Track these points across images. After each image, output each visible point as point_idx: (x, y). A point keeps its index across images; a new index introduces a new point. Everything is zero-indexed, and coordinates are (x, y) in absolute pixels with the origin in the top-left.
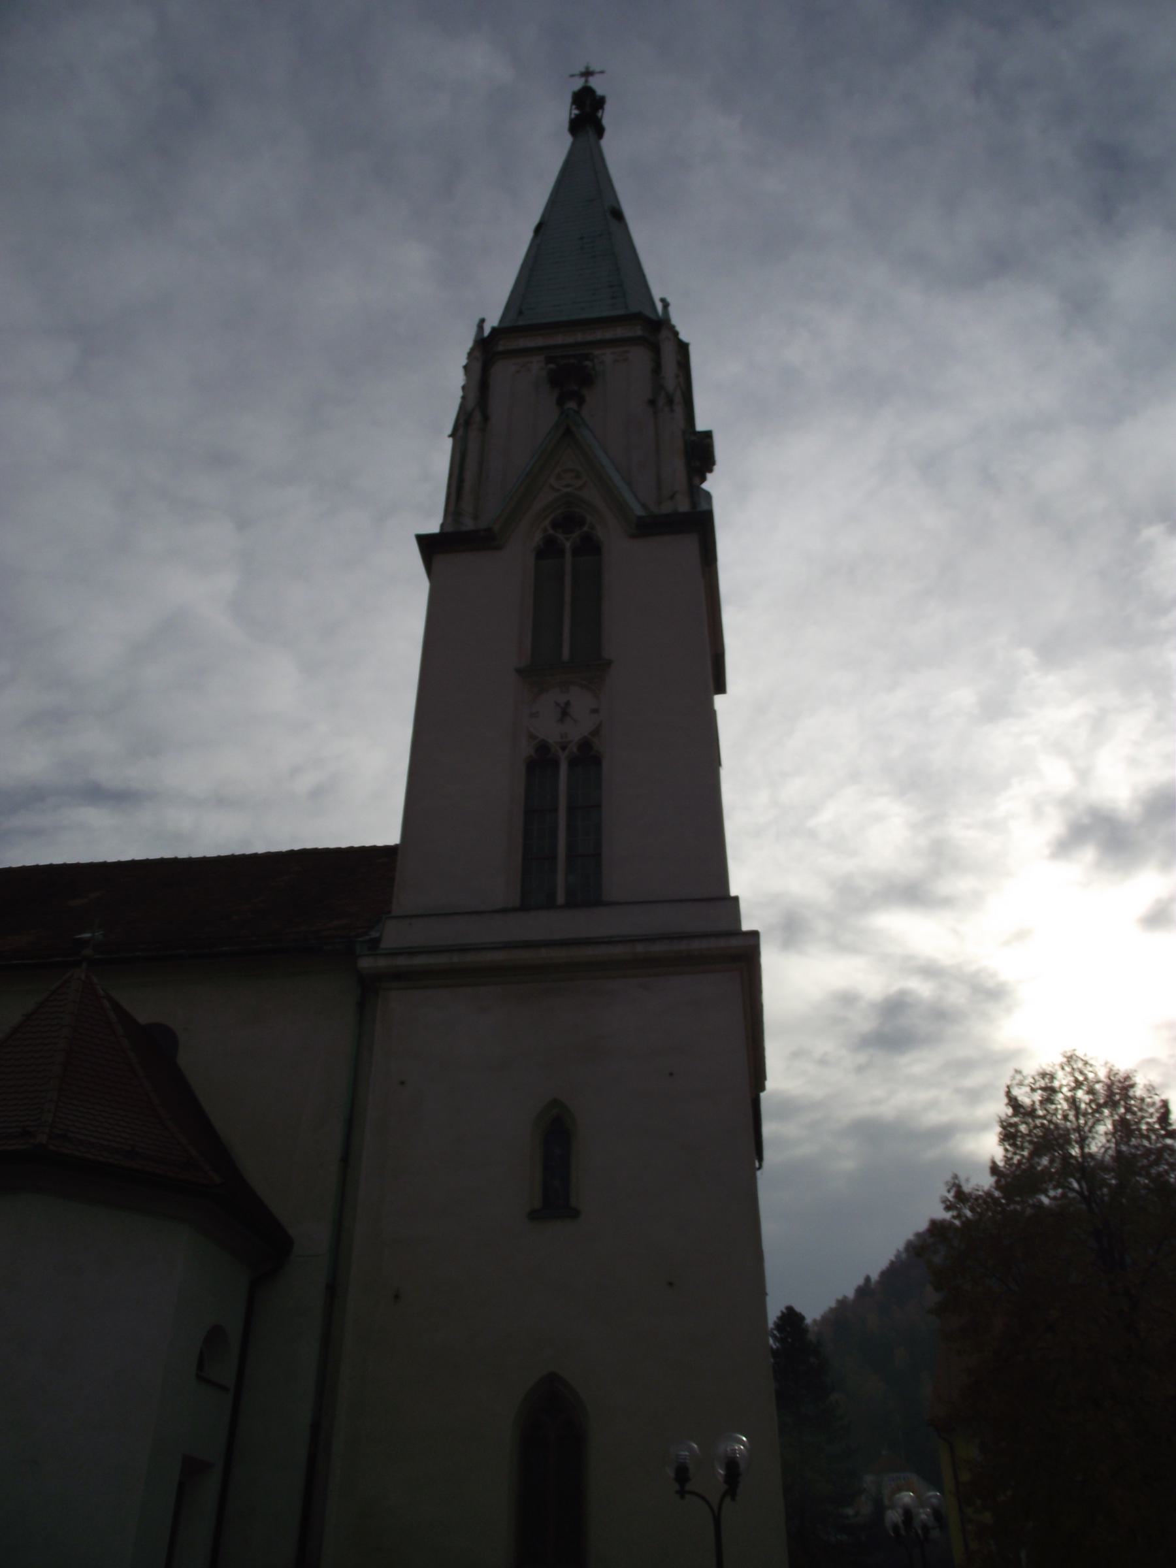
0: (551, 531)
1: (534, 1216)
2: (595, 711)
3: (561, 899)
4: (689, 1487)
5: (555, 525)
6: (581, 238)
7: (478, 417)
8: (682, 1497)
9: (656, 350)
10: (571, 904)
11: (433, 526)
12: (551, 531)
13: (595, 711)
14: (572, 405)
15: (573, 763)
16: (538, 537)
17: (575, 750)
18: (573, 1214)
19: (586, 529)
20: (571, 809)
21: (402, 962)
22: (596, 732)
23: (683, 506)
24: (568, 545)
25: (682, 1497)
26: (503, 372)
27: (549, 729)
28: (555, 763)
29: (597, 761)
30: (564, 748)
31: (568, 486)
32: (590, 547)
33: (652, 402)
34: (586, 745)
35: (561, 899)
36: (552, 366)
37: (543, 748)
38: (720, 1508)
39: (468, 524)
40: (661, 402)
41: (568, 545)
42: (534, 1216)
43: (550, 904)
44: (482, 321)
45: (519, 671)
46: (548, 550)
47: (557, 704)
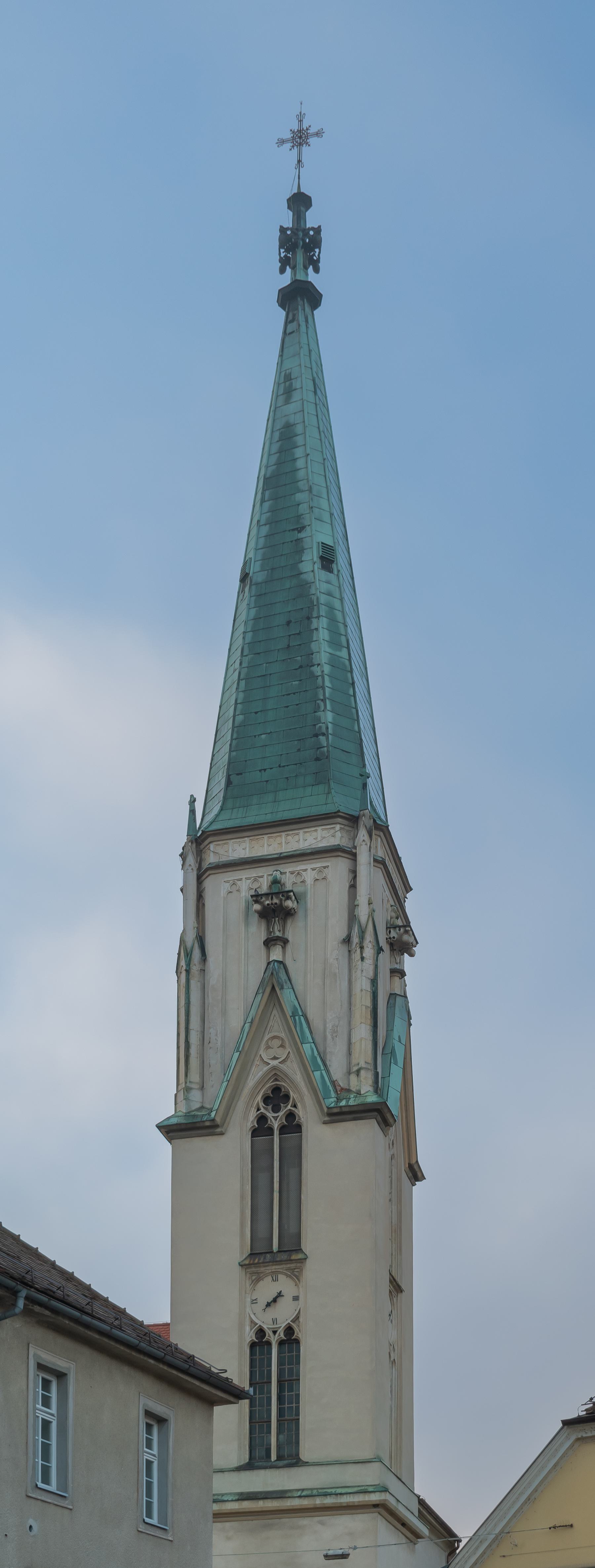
3: (274, 1457)
5: (266, 1100)
7: (197, 953)
12: (262, 1110)
13: (296, 1298)
16: (253, 1115)
17: (282, 1335)
19: (289, 1107)
20: (280, 1382)
22: (297, 1318)
29: (297, 1342)
30: (275, 1332)
31: (275, 1058)
32: (292, 1126)
33: (347, 940)
34: (289, 1330)
35: (274, 1457)
40: (355, 940)
46: (261, 1128)
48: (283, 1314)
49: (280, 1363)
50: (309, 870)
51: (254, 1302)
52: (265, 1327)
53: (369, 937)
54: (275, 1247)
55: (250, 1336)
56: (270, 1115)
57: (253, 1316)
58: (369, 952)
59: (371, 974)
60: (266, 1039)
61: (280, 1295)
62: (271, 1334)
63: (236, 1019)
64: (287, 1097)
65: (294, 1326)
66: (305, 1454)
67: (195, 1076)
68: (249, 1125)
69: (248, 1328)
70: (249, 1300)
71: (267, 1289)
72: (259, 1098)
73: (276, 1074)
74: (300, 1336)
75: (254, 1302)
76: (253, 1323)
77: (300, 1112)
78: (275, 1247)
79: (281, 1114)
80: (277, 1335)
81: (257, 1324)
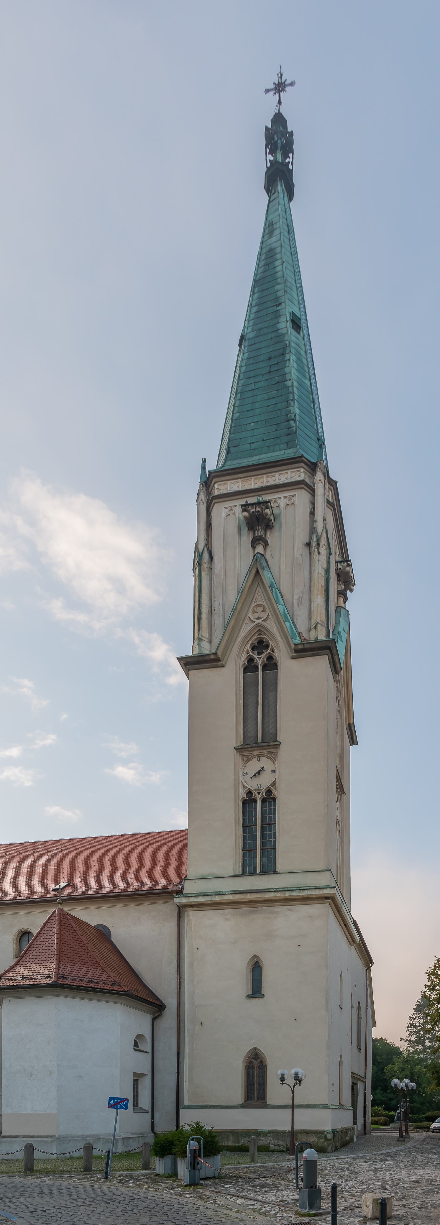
0: (251, 653)
3: (258, 870)
9: (312, 491)
10: (263, 872)
12: (251, 653)
13: (273, 772)
14: (260, 549)
15: (264, 801)
16: (244, 656)
17: (264, 794)
19: (269, 651)
21: (193, 900)
22: (274, 784)
23: (322, 636)
27: (253, 785)
30: (259, 793)
33: (309, 545)
35: (258, 870)
36: (246, 514)
39: (206, 649)
40: (314, 543)
41: (260, 664)
43: (253, 873)
44: (204, 461)
45: (236, 749)
48: (265, 781)
51: (245, 774)
52: (252, 789)
53: (323, 542)
54: (259, 739)
55: (242, 794)
58: (323, 550)
59: (325, 566)
61: (262, 769)
63: (232, 596)
65: (273, 789)
66: (278, 868)
67: (205, 633)
68: (242, 663)
69: (241, 790)
70: (241, 773)
71: (254, 766)
73: (260, 629)
74: (276, 794)
75: (245, 774)
76: (244, 787)
77: (276, 655)
78: (259, 739)
79: (263, 656)
80: (260, 794)
81: (247, 787)
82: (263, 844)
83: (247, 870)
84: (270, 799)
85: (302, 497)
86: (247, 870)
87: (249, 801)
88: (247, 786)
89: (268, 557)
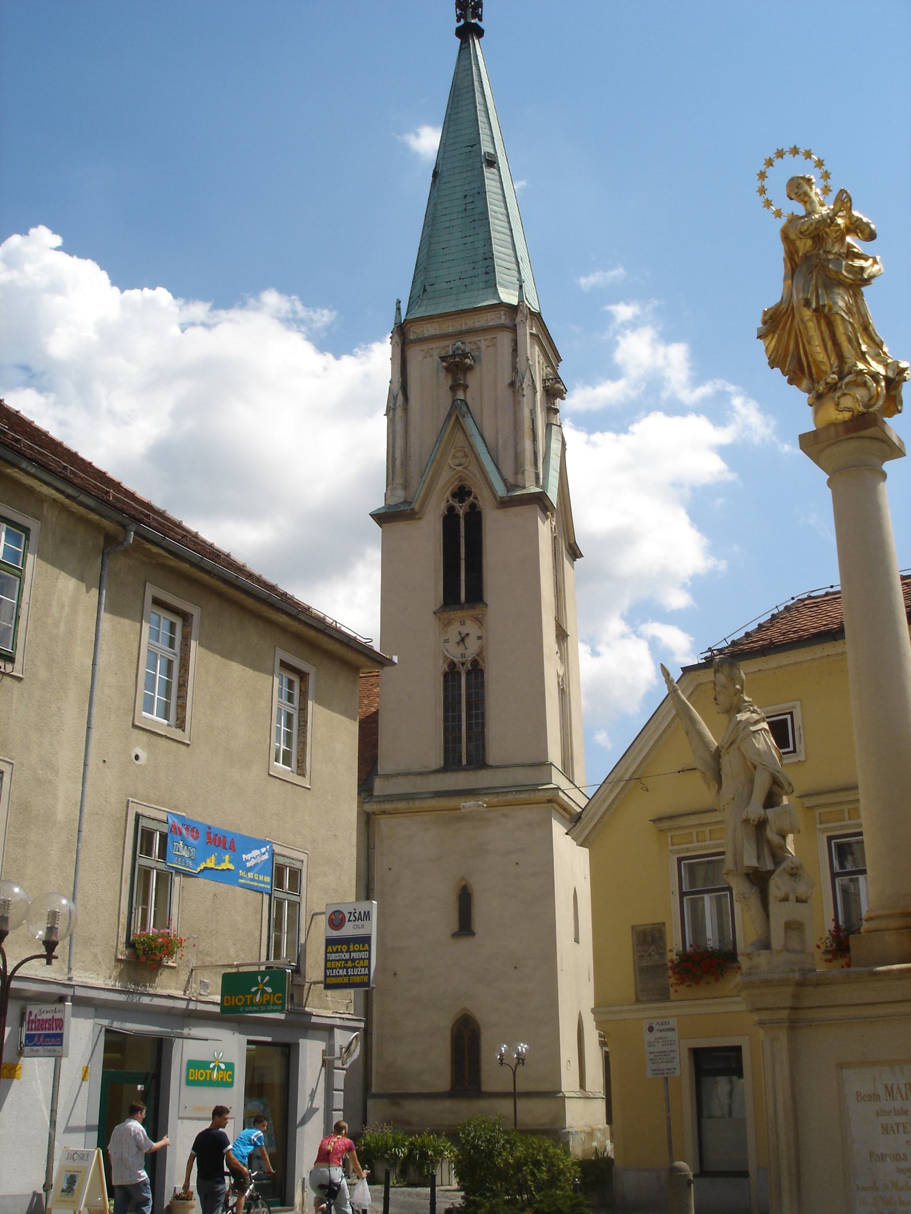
0: (451, 502)
1: (455, 935)
2: (480, 638)
3: (464, 762)
4: (504, 1062)
5: (454, 495)
6: (465, 196)
8: (502, 1065)
11: (379, 503)
12: (451, 502)
13: (480, 638)
15: (468, 673)
17: (469, 666)
18: (473, 934)
19: (471, 499)
22: (480, 653)
24: (461, 512)
25: (502, 1065)
26: (416, 355)
27: (455, 652)
28: (459, 674)
29: (482, 672)
31: (459, 465)
34: (475, 663)
35: (464, 762)
37: (452, 665)
38: (516, 1069)
41: (461, 512)
42: (455, 935)
47: (460, 633)
49: (468, 688)
50: (483, 341)
52: (455, 660)
55: (444, 667)
56: (457, 505)
57: (445, 652)
60: (453, 451)
62: (460, 666)
64: (469, 493)
66: (491, 760)
68: (441, 512)
72: (448, 494)
76: (446, 658)
82: (469, 727)
83: (451, 763)
84: (476, 671)
85: (505, 339)
86: (451, 763)
87: (451, 675)
88: (449, 656)
89: (469, 401)
